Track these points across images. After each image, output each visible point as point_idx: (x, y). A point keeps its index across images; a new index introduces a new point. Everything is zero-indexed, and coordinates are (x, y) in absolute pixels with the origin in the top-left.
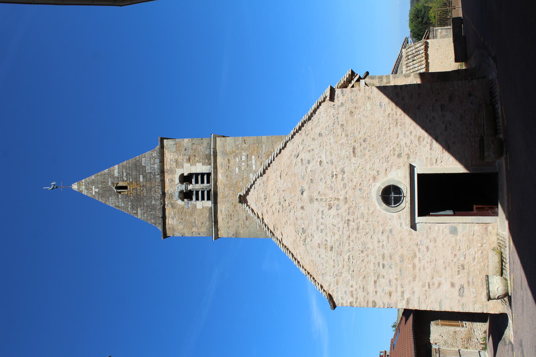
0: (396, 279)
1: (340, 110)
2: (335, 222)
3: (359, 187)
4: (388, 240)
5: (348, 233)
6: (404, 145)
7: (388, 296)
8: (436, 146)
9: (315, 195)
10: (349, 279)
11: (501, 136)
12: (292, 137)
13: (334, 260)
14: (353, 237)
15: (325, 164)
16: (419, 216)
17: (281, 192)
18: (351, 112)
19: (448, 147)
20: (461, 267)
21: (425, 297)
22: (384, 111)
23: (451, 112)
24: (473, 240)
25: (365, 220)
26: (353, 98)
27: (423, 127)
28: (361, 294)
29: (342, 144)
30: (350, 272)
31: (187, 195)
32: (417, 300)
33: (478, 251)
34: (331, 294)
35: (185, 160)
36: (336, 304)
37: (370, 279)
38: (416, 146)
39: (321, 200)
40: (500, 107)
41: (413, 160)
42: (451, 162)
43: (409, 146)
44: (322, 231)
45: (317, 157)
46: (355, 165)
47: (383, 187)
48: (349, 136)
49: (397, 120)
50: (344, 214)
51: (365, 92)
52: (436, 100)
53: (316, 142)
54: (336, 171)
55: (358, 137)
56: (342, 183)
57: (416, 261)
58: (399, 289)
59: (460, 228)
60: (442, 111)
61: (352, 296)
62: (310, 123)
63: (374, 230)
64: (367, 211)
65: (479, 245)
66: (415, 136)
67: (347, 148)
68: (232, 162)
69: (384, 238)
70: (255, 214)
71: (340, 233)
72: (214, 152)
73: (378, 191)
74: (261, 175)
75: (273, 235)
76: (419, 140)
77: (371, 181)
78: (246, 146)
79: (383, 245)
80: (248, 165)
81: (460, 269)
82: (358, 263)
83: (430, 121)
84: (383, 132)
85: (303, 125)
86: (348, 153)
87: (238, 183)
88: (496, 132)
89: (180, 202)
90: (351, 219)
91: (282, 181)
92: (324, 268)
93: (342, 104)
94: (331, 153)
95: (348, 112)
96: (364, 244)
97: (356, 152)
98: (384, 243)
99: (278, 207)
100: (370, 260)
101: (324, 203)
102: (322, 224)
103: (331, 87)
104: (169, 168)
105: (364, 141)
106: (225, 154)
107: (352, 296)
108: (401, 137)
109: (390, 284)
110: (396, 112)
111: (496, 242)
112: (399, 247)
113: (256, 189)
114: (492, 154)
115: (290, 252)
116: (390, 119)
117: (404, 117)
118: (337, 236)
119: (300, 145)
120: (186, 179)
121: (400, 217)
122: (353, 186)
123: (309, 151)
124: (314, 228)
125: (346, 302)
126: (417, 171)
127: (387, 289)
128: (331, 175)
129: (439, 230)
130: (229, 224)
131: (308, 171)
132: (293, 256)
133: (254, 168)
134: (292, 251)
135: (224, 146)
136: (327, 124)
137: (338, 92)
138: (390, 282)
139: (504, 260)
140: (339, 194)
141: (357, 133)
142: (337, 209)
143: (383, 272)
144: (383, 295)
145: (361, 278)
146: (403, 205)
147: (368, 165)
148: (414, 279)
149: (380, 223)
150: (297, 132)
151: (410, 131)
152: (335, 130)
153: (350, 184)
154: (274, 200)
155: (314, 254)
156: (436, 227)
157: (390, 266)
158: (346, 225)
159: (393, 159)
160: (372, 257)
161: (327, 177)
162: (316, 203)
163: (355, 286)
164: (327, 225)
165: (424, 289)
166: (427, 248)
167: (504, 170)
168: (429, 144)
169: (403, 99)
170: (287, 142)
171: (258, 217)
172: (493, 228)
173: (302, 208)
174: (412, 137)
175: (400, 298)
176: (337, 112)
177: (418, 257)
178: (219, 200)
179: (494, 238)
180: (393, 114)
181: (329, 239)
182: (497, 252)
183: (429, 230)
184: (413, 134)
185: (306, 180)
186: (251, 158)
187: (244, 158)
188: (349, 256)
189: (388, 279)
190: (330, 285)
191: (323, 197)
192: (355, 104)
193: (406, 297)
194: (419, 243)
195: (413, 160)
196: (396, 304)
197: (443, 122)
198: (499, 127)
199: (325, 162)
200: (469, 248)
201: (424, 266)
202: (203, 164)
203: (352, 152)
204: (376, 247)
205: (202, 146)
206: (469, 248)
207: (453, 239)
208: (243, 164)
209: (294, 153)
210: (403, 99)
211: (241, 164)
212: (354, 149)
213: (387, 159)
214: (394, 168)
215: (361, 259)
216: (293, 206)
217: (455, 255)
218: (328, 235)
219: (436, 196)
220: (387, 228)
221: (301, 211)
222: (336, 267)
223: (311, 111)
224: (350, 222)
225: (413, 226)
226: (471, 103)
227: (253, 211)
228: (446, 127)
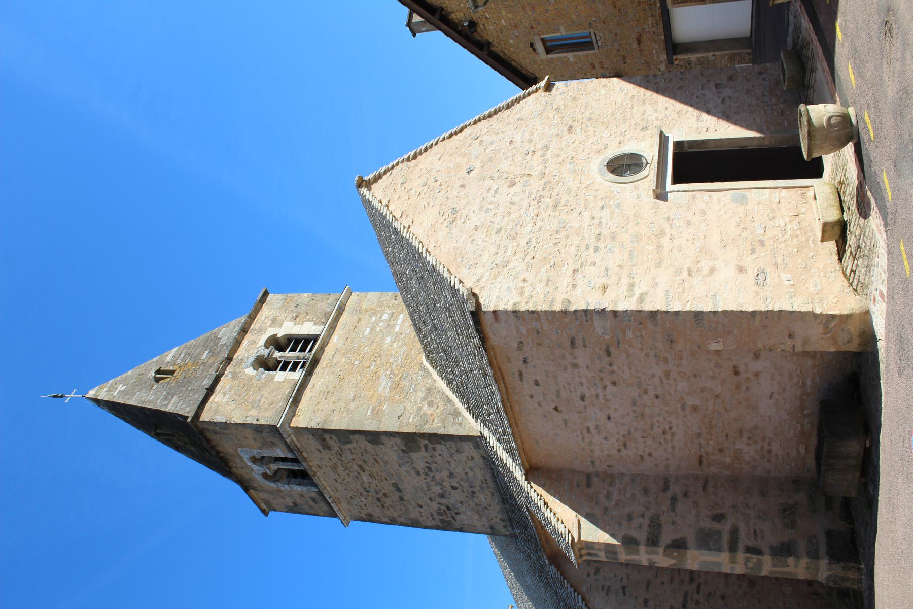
31: (265, 364)
33: (791, 221)
35: (289, 318)
37: (565, 268)
44: (487, 210)
58: (625, 281)
61: (522, 294)
68: (362, 323)
74: (408, 160)
85: (495, 112)
89: (250, 371)
104: (257, 327)
106: (358, 310)
107: (522, 294)
120: (278, 343)
126: (674, 137)
130: (320, 407)
138: (607, 270)
150: (484, 118)
175: (626, 294)
178: (318, 369)
181: (497, 220)
186: (397, 317)
193: (637, 291)
202: (315, 324)
205: (327, 303)
225: (661, 195)
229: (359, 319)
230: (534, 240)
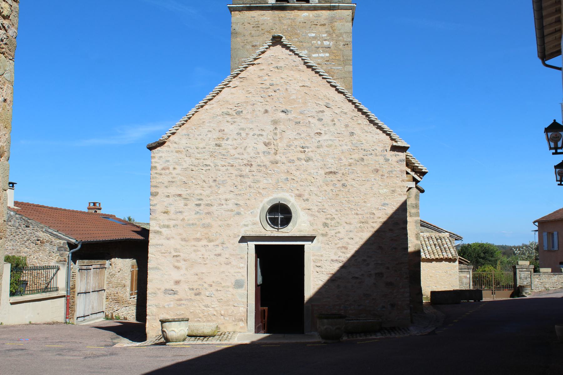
0: (183, 220)
1: (380, 157)
2: (249, 150)
3: (290, 177)
4: (228, 211)
5: (236, 164)
6: (337, 231)
7: (164, 210)
8: (336, 267)
9: (281, 127)
10: (183, 165)
11: (345, 338)
12: (350, 101)
13: (205, 148)
14: (231, 170)
15: (318, 139)
16: (256, 246)
17: (285, 87)
18: (377, 171)
19: (334, 279)
20: (197, 292)
21: (163, 251)
22: (378, 209)
23: (374, 284)
24: (229, 305)
25: (252, 184)
26: (394, 173)
27: (357, 253)
28: (165, 179)
29: (341, 159)
30: (191, 167)
32: (160, 242)
33: (216, 311)
34: (166, 144)
36: (154, 151)
37: (184, 189)
38: (336, 244)
39: (276, 134)
40: (378, 337)
41: (320, 240)
42: (317, 283)
43: (336, 236)
45: (326, 129)
46: (315, 174)
47: (289, 206)
48: (349, 167)
49: (367, 223)
50: (258, 160)
51: (400, 187)
52: (388, 268)
53: (344, 129)
54: (309, 152)
55: (348, 178)
56: (295, 158)
57: (204, 242)
58: (172, 223)
59: (242, 291)
60: (376, 274)
61: (163, 169)
62: (366, 122)
63: (240, 195)
64: (261, 187)
65: (223, 312)
66: (348, 243)
67: (335, 165)
69: (231, 206)
70: (260, 55)
71: (237, 156)
72: (334, 6)
73: (285, 200)
74: (305, 63)
75: (234, 77)
76: (343, 247)
77: (297, 192)
78: (341, 46)
79: (223, 205)
80: (318, 48)
81: (195, 291)
82: (202, 176)
83: (365, 260)
84: (353, 207)
85: (364, 113)
86: (330, 166)
87: (296, 36)
88: (350, 333)
90: (252, 169)
91: (298, 88)
92: (196, 136)
93: (387, 160)
94: (330, 146)
95: (378, 167)
96: (224, 183)
97: (331, 175)
98: (225, 206)
99: (267, 83)
100: (205, 189)
101: (271, 137)
102: (247, 134)
103: (408, 147)
105: (343, 185)
106: (332, 20)
107: (163, 169)
108: (347, 227)
109: (177, 212)
110: (376, 222)
111: (225, 331)
112: (220, 223)
113: (288, 56)
114: (325, 327)
115: (214, 96)
116: (368, 216)
117: (370, 231)
118: (232, 152)
119: (340, 110)
121: (254, 224)
122: (291, 171)
123: (333, 121)
124: (243, 125)
125: (156, 162)
127: (172, 209)
128: (304, 145)
129: (240, 268)
130: (247, 25)
131: (310, 119)
132: (210, 100)
133: (314, 55)
134: (215, 99)
135: (341, 19)
136: (364, 142)
137: (402, 156)
138: (180, 212)
139: (206, 339)
140: (281, 155)
141: (353, 176)
142: (264, 152)
143: (191, 205)
144: (165, 204)
145: (184, 179)
146: (268, 228)
147: (315, 189)
148: (184, 240)
149: (248, 202)
150: (356, 107)
151: (354, 237)
152: (357, 151)
153: (293, 168)
154: (276, 79)
155: (212, 125)
156: (243, 265)
157: (198, 212)
158: (245, 162)
159: (322, 218)
160: (208, 192)
161: (302, 141)
162: (272, 127)
163: (174, 172)
164: (246, 141)
165: (172, 251)
166: (219, 255)
167: (307, 341)
168: (338, 259)
169: (390, 230)
170: (344, 95)
171: (255, 59)
172: (241, 328)
173: (266, 111)
174: (346, 240)
175: (162, 224)
176: (378, 154)
177: (209, 244)
178: (277, 12)
179: (230, 328)
180: (373, 218)
181: (230, 142)
182: (214, 331)
183: (240, 256)
184: (350, 241)
185: (299, 117)
186: (326, 52)
187: (326, 43)
188: (209, 165)
189: (183, 210)
190: (176, 143)
191: (279, 136)
192: (386, 175)
193: (163, 230)
194: (225, 246)
195: (320, 240)
196: (155, 219)
197: (363, 275)
198: (355, 336)
199: (320, 139)
200: (220, 300)
201: (198, 251)
203: (330, 170)
204: (220, 196)
206: (220, 300)
207: (230, 284)
208: (319, 42)
209: (331, 102)
210: (390, 230)
211: (319, 40)
212: (335, 173)
213: (322, 210)
214: (311, 219)
215: (206, 180)
216: (268, 100)
217: (211, 286)
218: (234, 142)
219: (279, 265)
220: (242, 209)
221: (263, 110)
222: (196, 150)
223: (381, 124)
224: (249, 167)
225: (244, 239)
226: (383, 307)
227: (263, 52)
228: (357, 278)
229: (324, 25)
230: (208, 168)
